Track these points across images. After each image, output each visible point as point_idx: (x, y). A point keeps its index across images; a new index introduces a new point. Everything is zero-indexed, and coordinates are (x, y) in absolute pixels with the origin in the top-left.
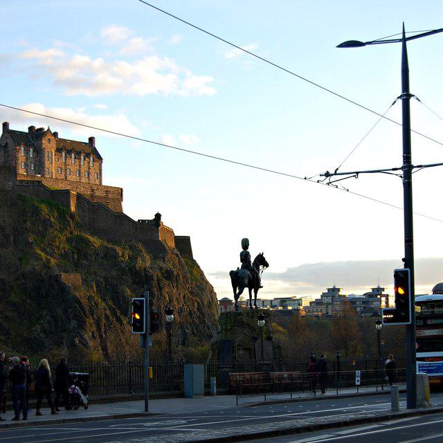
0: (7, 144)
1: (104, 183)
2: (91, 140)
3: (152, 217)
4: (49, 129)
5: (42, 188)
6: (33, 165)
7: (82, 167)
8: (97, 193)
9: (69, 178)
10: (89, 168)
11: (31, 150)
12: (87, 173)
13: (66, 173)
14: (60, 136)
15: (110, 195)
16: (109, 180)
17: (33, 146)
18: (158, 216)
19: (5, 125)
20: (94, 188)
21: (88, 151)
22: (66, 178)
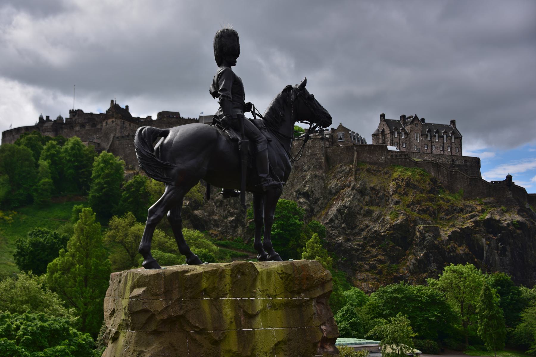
0: (383, 130)
1: (463, 155)
2: (453, 122)
3: (503, 178)
4: (416, 116)
5: (408, 160)
6: (404, 144)
7: (445, 144)
8: (457, 163)
9: (434, 152)
10: (451, 144)
11: (403, 133)
12: (449, 148)
13: (432, 149)
14: (426, 121)
15: (468, 164)
19: (383, 116)
20: (455, 158)
22: (432, 152)
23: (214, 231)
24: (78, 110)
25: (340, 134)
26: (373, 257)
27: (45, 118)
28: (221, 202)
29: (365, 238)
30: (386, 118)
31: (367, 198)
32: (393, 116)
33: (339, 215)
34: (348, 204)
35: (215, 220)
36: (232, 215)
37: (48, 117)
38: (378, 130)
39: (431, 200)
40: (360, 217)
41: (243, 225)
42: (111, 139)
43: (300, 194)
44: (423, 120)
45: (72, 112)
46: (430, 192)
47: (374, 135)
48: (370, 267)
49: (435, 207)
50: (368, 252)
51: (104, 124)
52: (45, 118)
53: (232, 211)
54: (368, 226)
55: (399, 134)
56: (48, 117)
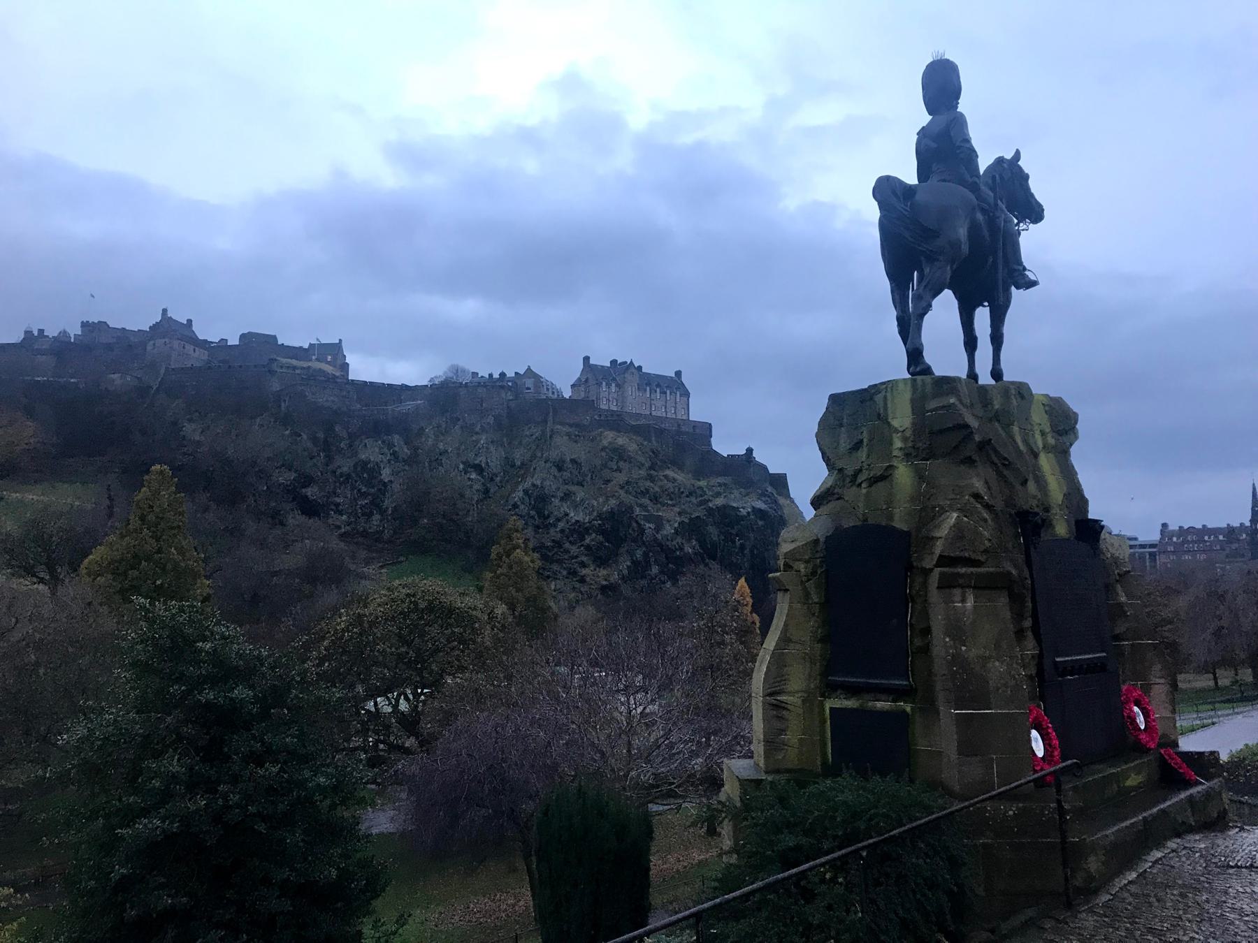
2: (678, 374)
8: (683, 429)
16: (697, 413)
17: (614, 379)
18: (750, 451)
19: (586, 359)
21: (674, 386)
23: (335, 519)
24: (100, 322)
25: (529, 383)
26: (573, 557)
27: (36, 333)
28: (348, 476)
29: (562, 531)
30: (592, 362)
31: (566, 474)
32: (601, 359)
33: (527, 499)
34: (538, 483)
35: (337, 505)
36: (364, 495)
37: (41, 331)
38: (579, 379)
39: (651, 478)
40: (556, 502)
41: (382, 512)
42: (162, 371)
43: (470, 466)
44: (640, 368)
45: (85, 325)
46: (651, 468)
47: (573, 386)
48: (569, 573)
49: (657, 489)
50: (567, 551)
51: (149, 348)
52: (36, 333)
53: (364, 489)
54: (567, 515)
55: (608, 385)
56: (41, 331)
